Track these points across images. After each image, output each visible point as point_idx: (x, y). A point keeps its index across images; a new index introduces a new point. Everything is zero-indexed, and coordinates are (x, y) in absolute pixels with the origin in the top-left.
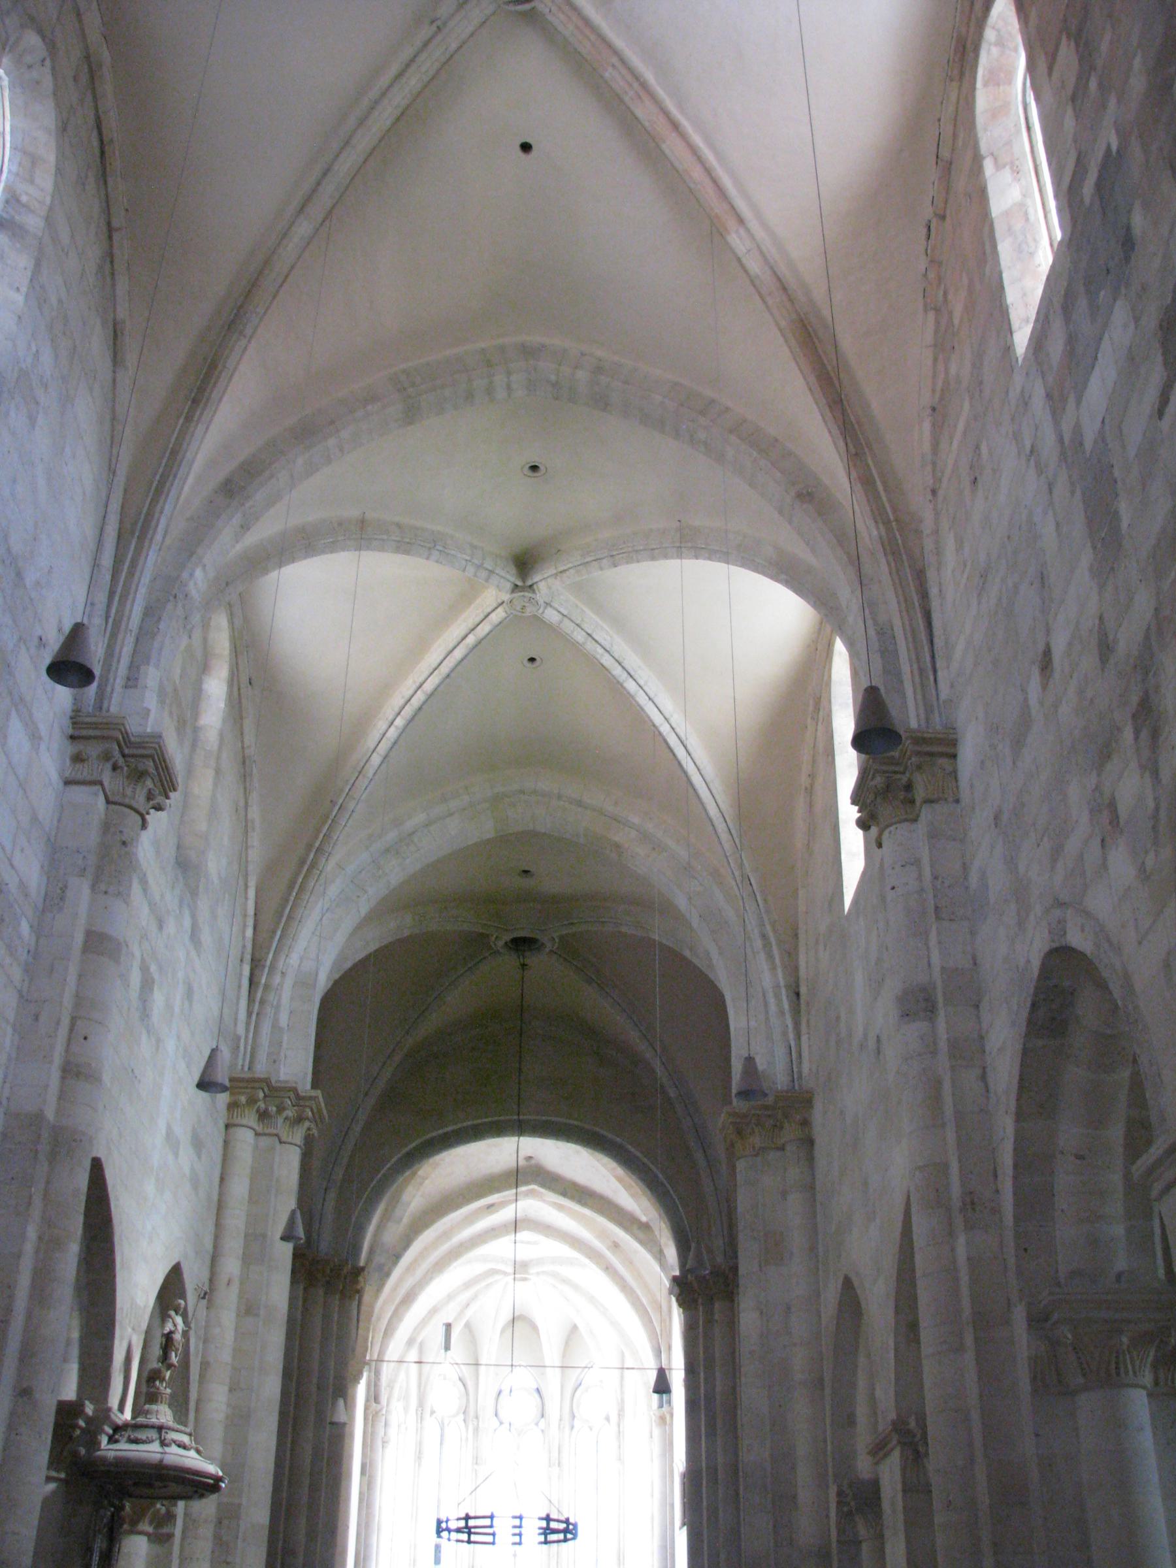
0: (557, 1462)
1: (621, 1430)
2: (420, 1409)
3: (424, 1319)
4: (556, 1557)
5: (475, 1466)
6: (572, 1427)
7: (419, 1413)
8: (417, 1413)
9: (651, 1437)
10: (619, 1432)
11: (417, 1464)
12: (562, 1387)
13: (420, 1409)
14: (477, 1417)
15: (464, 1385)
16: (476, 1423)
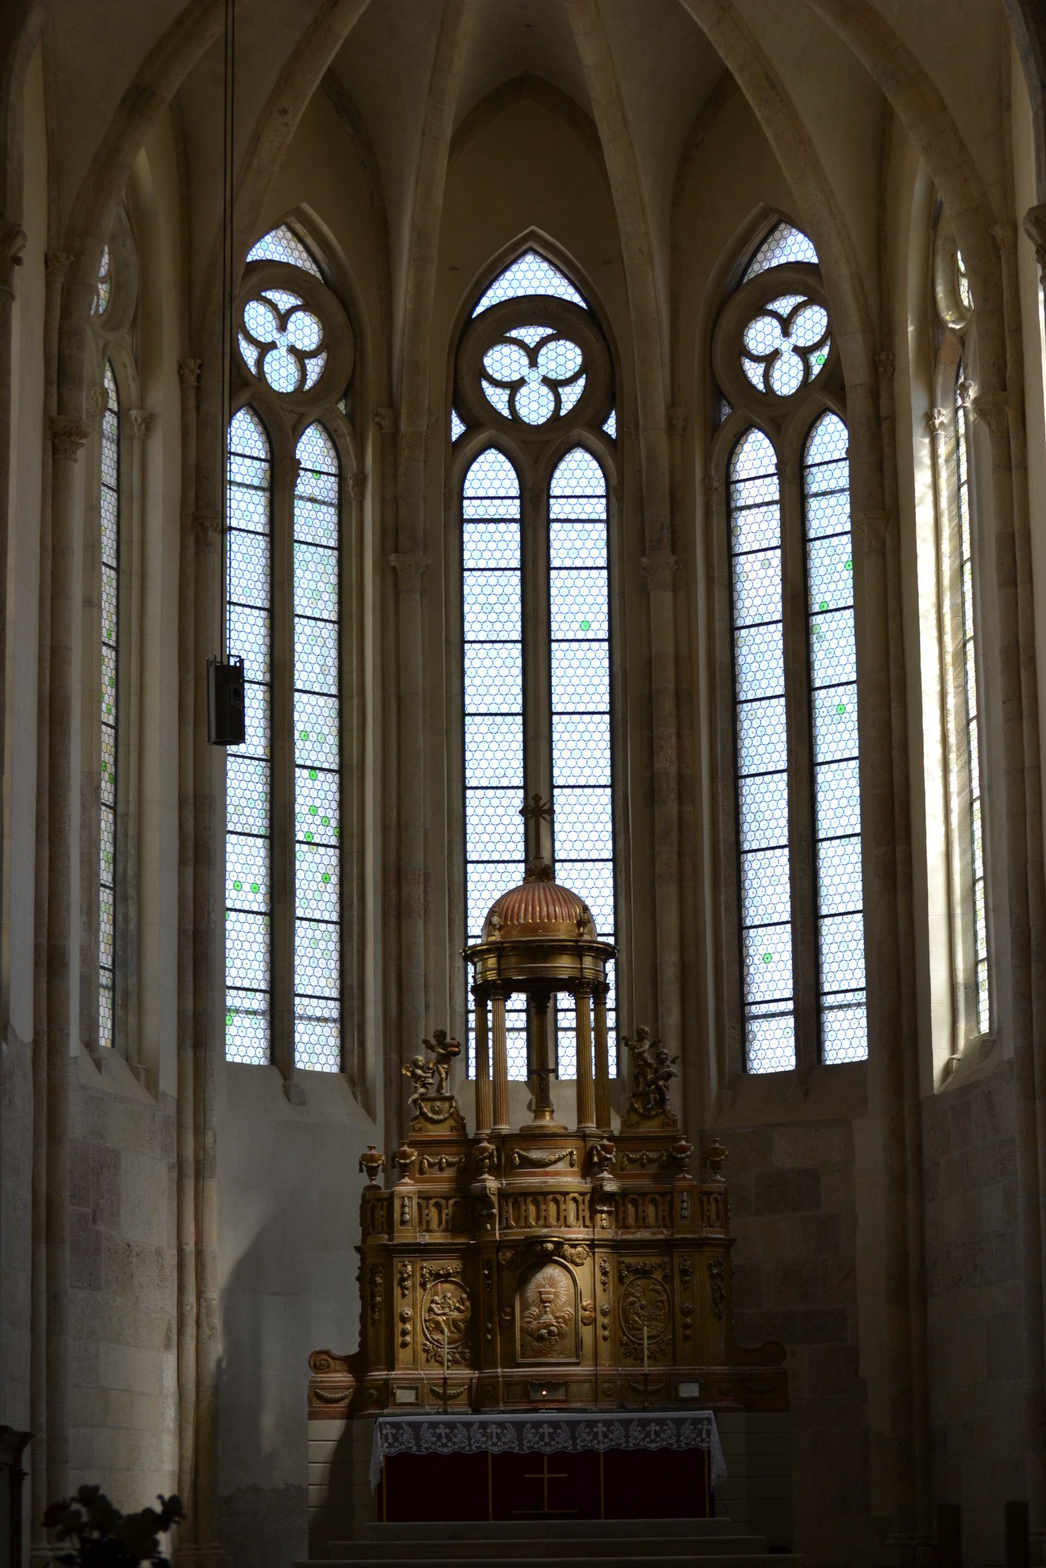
0: (666, 536)
1: (884, 412)
2: (192, 363)
3: (179, 22)
4: (674, 836)
5: (392, 558)
6: (714, 427)
7: (191, 379)
8: (181, 377)
9: (1004, 388)
10: (878, 419)
11: (191, 542)
12: (674, 298)
13: (192, 363)
14: (392, 404)
15: (346, 304)
16: (386, 423)
